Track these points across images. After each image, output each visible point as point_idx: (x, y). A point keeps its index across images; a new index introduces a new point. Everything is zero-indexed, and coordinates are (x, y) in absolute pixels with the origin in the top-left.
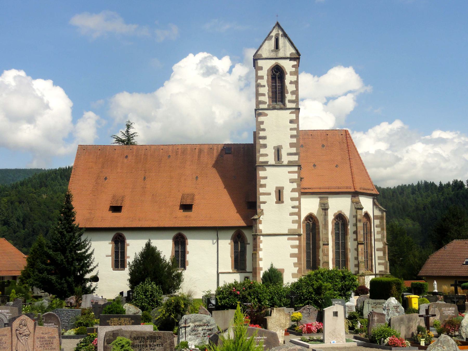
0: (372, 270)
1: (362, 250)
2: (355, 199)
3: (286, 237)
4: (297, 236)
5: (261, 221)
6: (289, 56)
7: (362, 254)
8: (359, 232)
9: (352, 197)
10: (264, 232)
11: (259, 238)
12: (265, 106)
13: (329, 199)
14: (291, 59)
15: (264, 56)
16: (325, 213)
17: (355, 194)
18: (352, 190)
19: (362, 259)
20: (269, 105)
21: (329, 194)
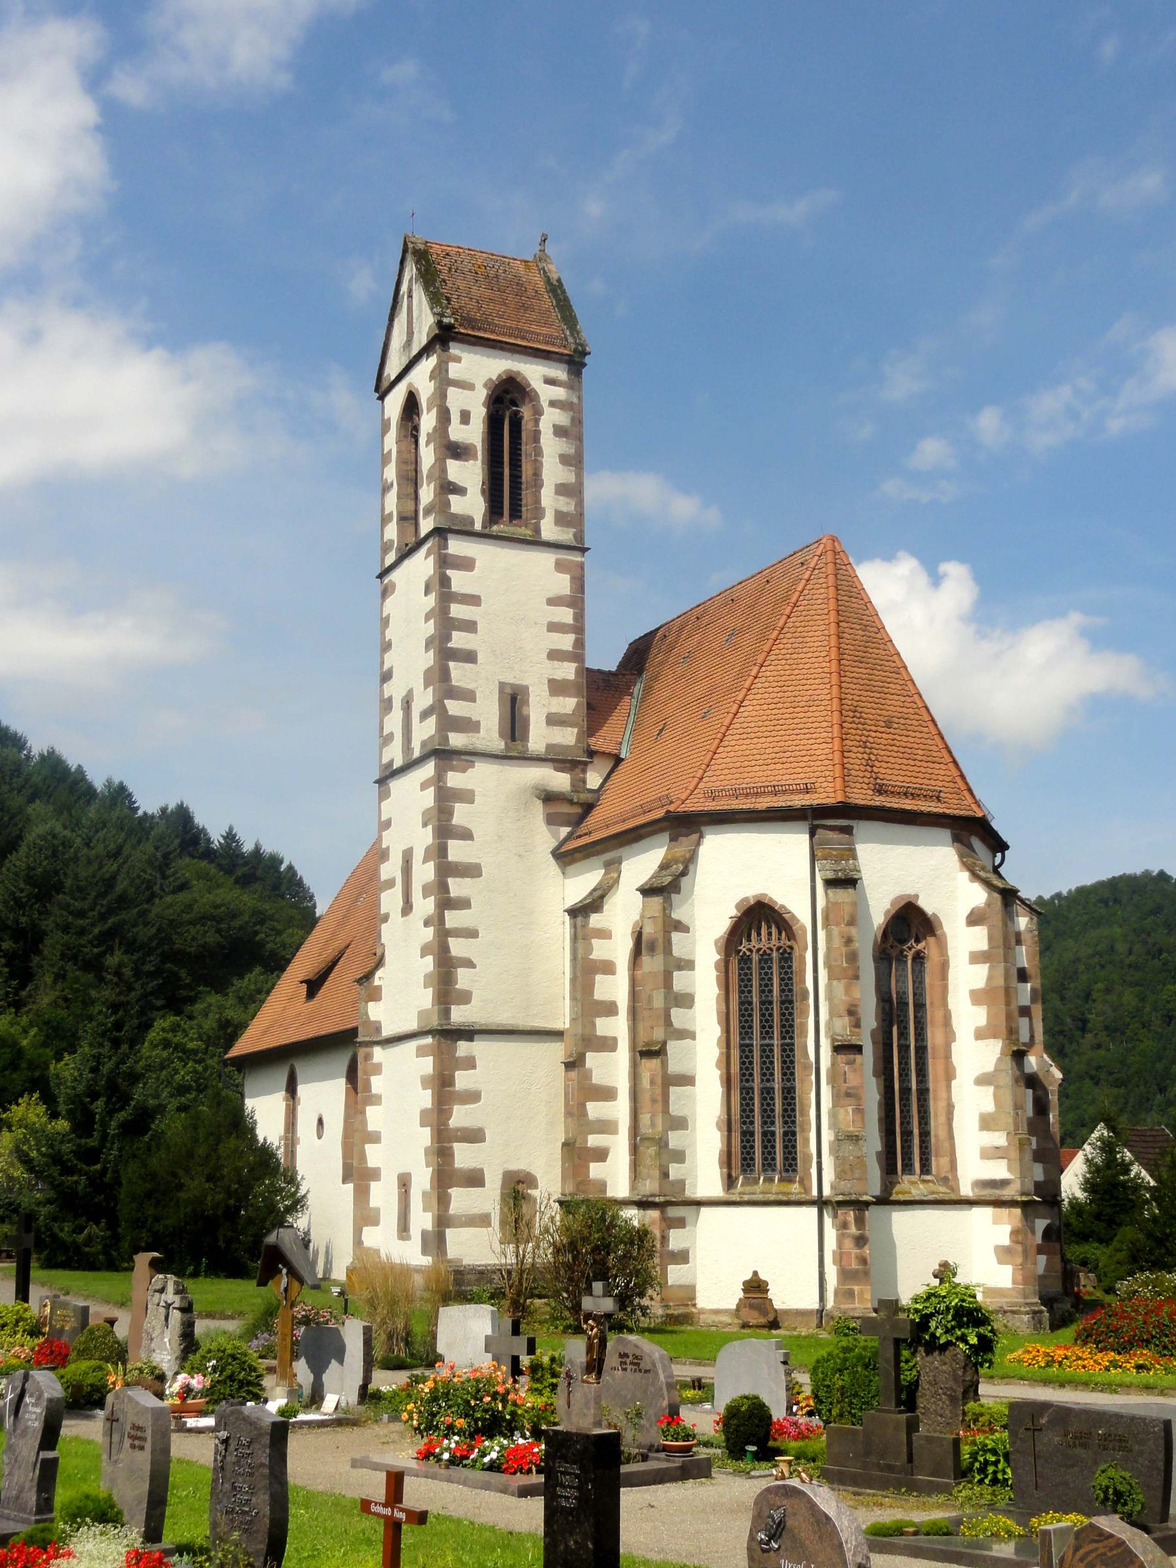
0: (805, 1184)
1: (652, 1082)
2: (682, 848)
3: (412, 1045)
4: (429, 1040)
5: (379, 988)
6: (424, 341)
7: (654, 1101)
8: (650, 997)
9: (671, 840)
10: (386, 1032)
11: (368, 1057)
12: (391, 558)
13: (625, 866)
14: (426, 351)
15: (393, 378)
16: (574, 926)
17: (685, 825)
18: (659, 814)
19: (653, 1125)
20: (398, 549)
21: (622, 845)
